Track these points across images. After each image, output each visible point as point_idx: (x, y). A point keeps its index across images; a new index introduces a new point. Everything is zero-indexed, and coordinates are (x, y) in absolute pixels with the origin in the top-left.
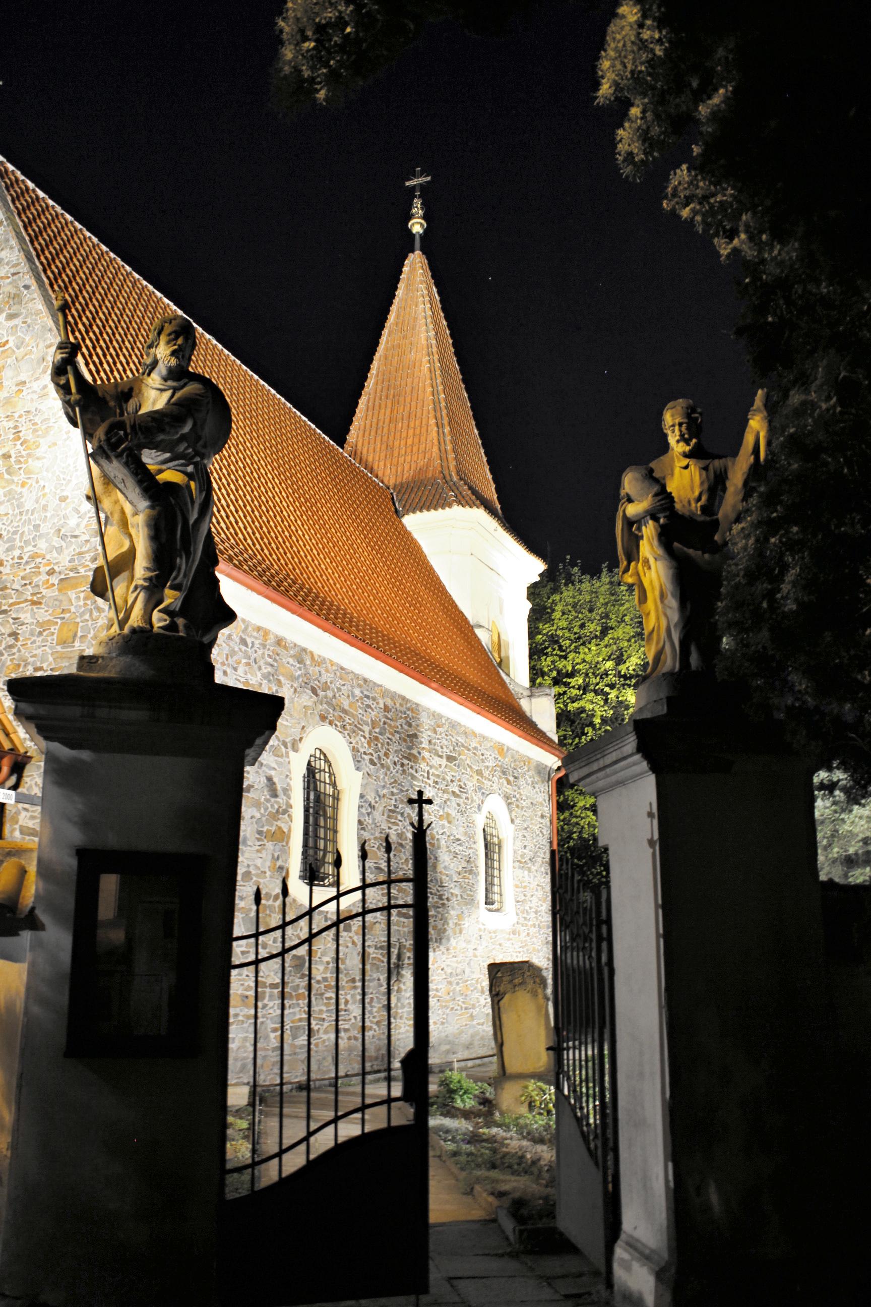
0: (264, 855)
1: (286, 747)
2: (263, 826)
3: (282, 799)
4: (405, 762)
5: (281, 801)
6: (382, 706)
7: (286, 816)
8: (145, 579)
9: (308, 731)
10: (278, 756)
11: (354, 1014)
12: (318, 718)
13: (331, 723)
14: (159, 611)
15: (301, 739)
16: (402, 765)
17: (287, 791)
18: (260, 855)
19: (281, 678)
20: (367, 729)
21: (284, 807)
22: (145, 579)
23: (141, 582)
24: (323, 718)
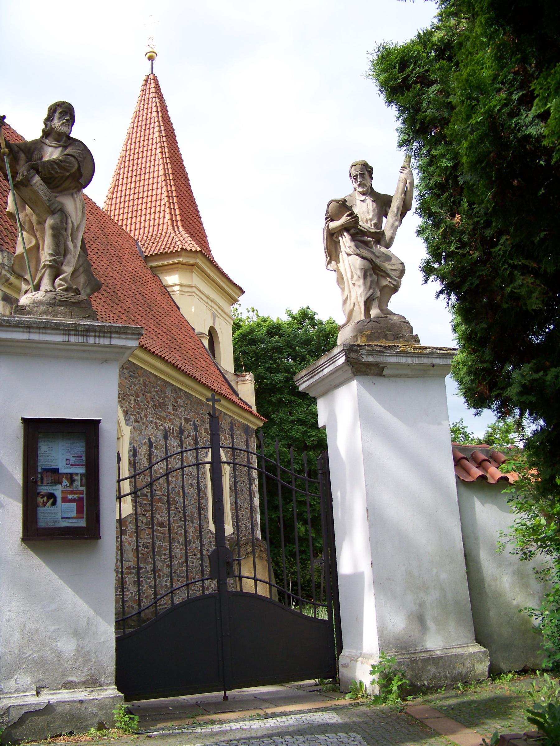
4: (157, 421)
6: (141, 382)
8: (50, 261)
11: (131, 591)
14: (60, 280)
16: (156, 423)
20: (132, 398)
23: (47, 263)
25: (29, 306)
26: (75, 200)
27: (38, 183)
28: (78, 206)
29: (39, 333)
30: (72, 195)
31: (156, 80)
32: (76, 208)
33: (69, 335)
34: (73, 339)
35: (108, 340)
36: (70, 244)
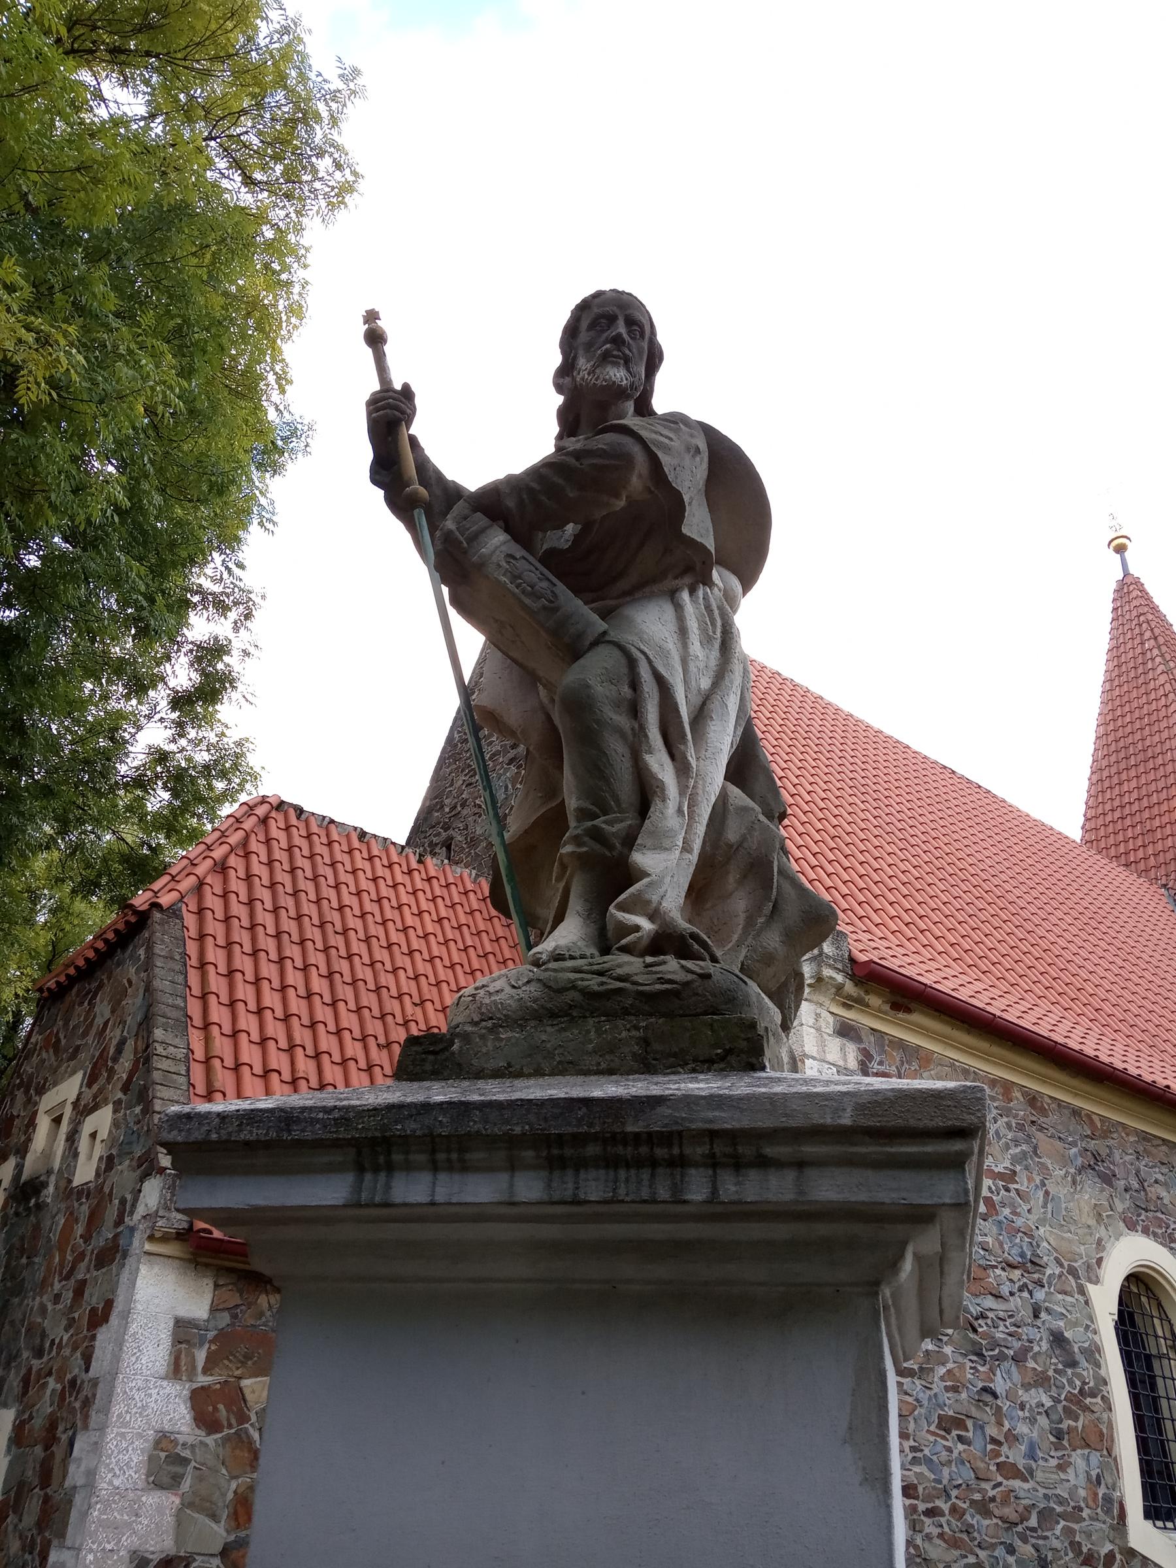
0: (1070, 1474)
1: (1077, 1277)
2: (1061, 1422)
3: (1085, 1369)
5: (1085, 1373)
7: (1098, 1400)
8: (577, 840)
9: (1108, 1246)
10: (1065, 1293)
12: (1122, 1224)
13: (1146, 1231)
15: (1099, 1261)
17: (1093, 1353)
18: (1063, 1476)
19: (1048, 1162)
21: (1092, 1384)
22: (577, 840)
24: (1131, 1226)
25: (466, 1037)
26: (678, 608)
27: (499, 557)
28: (693, 625)
29: (435, 1168)
30: (672, 595)
31: (1137, 582)
32: (683, 631)
33: (580, 1164)
34: (594, 1186)
35: (790, 1175)
36: (660, 765)
